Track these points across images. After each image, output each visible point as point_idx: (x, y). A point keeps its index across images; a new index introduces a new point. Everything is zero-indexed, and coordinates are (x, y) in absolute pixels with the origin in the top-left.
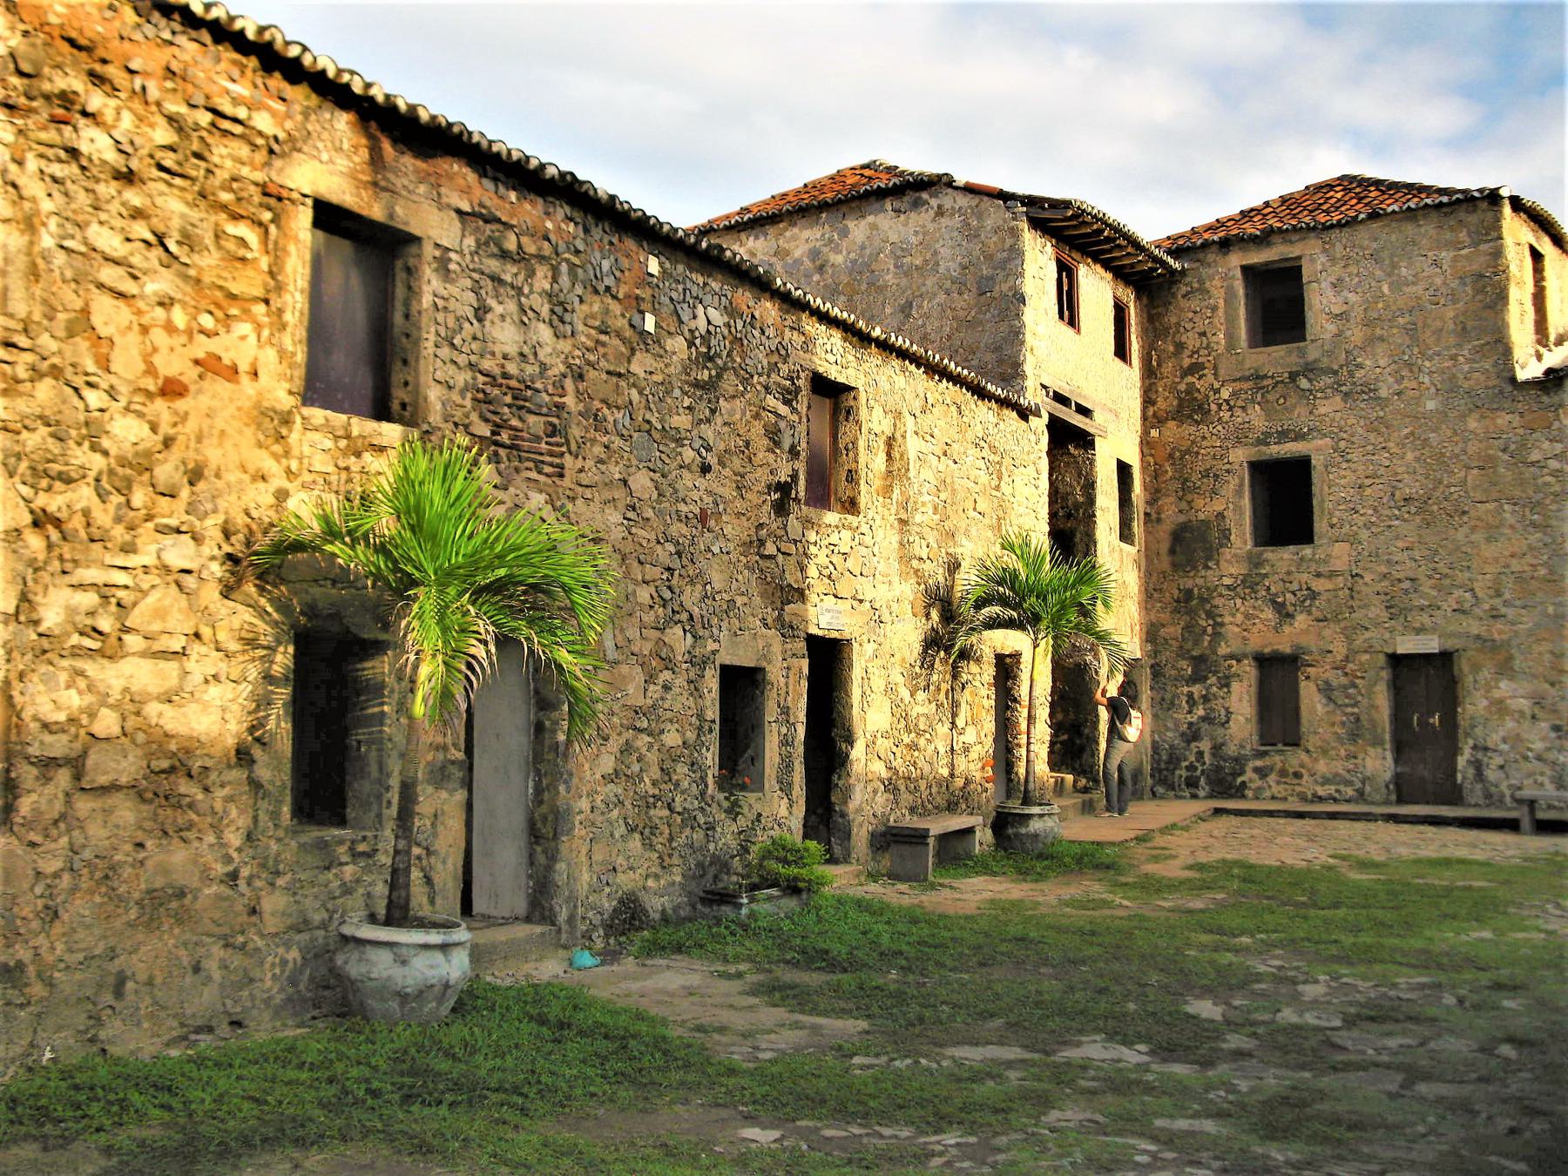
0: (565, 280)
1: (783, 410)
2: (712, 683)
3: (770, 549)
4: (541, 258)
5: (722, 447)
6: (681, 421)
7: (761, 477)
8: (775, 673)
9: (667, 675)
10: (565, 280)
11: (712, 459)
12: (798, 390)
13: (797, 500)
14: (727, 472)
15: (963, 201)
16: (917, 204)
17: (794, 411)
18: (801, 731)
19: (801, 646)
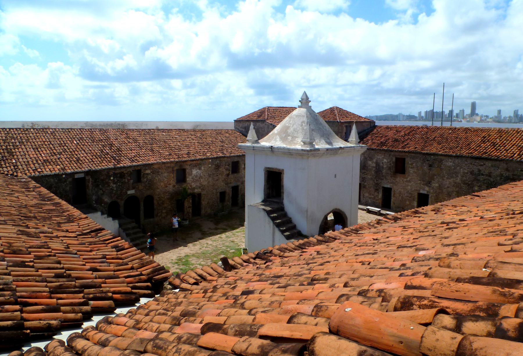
1: (227, 167)
2: (219, 194)
6: (214, 172)
7: (225, 174)
11: (218, 175)
16: (263, 123)
18: (231, 196)
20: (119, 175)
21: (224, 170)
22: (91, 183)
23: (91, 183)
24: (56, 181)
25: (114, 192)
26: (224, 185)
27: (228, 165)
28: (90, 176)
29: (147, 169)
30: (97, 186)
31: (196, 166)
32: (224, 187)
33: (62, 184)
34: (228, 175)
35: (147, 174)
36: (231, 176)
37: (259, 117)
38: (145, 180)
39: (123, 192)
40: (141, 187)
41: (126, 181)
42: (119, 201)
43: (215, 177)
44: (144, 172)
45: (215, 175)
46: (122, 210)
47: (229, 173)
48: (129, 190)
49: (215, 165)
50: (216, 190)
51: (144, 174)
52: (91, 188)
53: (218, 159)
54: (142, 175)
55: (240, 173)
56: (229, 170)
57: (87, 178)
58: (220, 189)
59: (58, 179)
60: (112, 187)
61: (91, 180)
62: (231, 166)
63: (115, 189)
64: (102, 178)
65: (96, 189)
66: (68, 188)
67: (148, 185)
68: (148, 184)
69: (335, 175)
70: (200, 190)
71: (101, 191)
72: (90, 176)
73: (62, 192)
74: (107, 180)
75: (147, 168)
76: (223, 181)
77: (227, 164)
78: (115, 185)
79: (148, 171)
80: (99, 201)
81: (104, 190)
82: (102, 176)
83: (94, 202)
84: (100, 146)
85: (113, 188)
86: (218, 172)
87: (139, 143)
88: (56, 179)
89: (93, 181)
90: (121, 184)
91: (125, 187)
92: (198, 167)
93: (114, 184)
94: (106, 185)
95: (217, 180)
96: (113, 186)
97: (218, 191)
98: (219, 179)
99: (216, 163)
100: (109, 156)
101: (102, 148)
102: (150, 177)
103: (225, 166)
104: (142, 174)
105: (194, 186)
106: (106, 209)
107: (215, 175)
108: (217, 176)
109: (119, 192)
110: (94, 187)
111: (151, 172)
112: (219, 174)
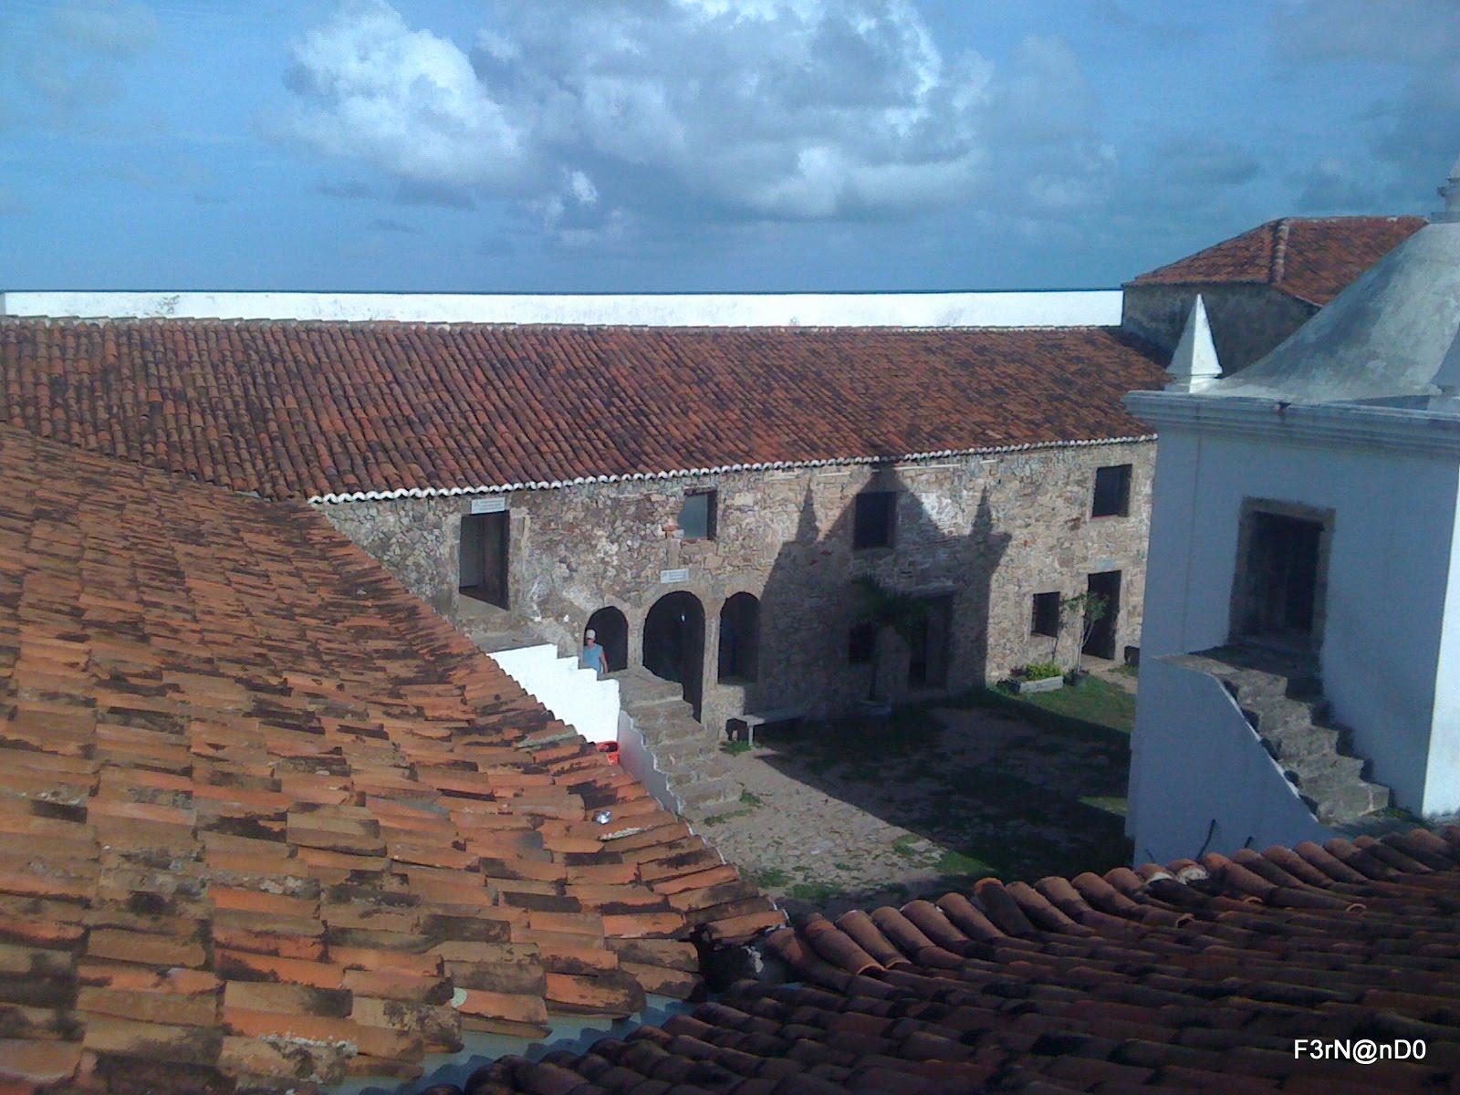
0: (956, 483)
1: (1076, 489)
2: (1028, 603)
3: (1067, 545)
4: (946, 478)
5: (1038, 514)
6: (1017, 511)
7: (1061, 520)
10: (956, 483)
11: (1032, 521)
12: (1086, 479)
13: (1085, 522)
14: (1041, 523)
15: (1279, 297)
17: (1083, 487)
19: (1086, 577)
20: (633, 509)
21: (1060, 503)
22: (527, 533)
23: (527, 533)
24: (405, 521)
25: (611, 572)
26: (1056, 565)
27: (1079, 483)
28: (524, 509)
29: (740, 491)
30: (550, 547)
32: (1055, 576)
33: (425, 533)
34: (1075, 524)
35: (739, 509)
37: (1241, 266)
38: (732, 531)
39: (643, 574)
40: (710, 554)
41: (660, 533)
42: (624, 607)
44: (728, 502)
45: (1019, 522)
46: (635, 643)
47: (1083, 514)
48: (666, 565)
49: (1021, 481)
50: (1020, 587)
51: (728, 507)
52: (525, 552)
53: (1035, 455)
54: (719, 513)
55: (1132, 519)
56: (1083, 505)
57: (516, 515)
58: (1034, 584)
59: (411, 514)
60: (606, 553)
61: (528, 522)
62: (1091, 484)
63: (615, 563)
64: (569, 517)
65: (545, 560)
66: (444, 551)
67: (742, 552)
68: (743, 546)
70: (950, 583)
71: (564, 566)
72: (524, 509)
73: (423, 562)
74: (589, 527)
75: (740, 485)
76: (1051, 549)
77: (1076, 476)
78: (615, 548)
79: (740, 500)
80: (550, 604)
81: (574, 565)
82: (569, 509)
83: (535, 607)
84: (572, 395)
85: (607, 559)
86: (1031, 511)
87: (717, 385)
88: (407, 515)
89: (537, 527)
90: (636, 545)
91: (652, 558)
92: (947, 485)
93: (612, 542)
94: (582, 546)
95: (1026, 543)
96: (608, 548)
97: (1026, 589)
98: (1034, 541)
99: (1028, 473)
100: (603, 435)
101: (577, 402)
102: (753, 519)
103: (1067, 484)
104: (721, 506)
105: (927, 566)
106: (577, 635)
107: (1019, 522)
108: (1028, 525)
109: (629, 573)
110: (538, 552)
111: (756, 503)
112: (1037, 520)
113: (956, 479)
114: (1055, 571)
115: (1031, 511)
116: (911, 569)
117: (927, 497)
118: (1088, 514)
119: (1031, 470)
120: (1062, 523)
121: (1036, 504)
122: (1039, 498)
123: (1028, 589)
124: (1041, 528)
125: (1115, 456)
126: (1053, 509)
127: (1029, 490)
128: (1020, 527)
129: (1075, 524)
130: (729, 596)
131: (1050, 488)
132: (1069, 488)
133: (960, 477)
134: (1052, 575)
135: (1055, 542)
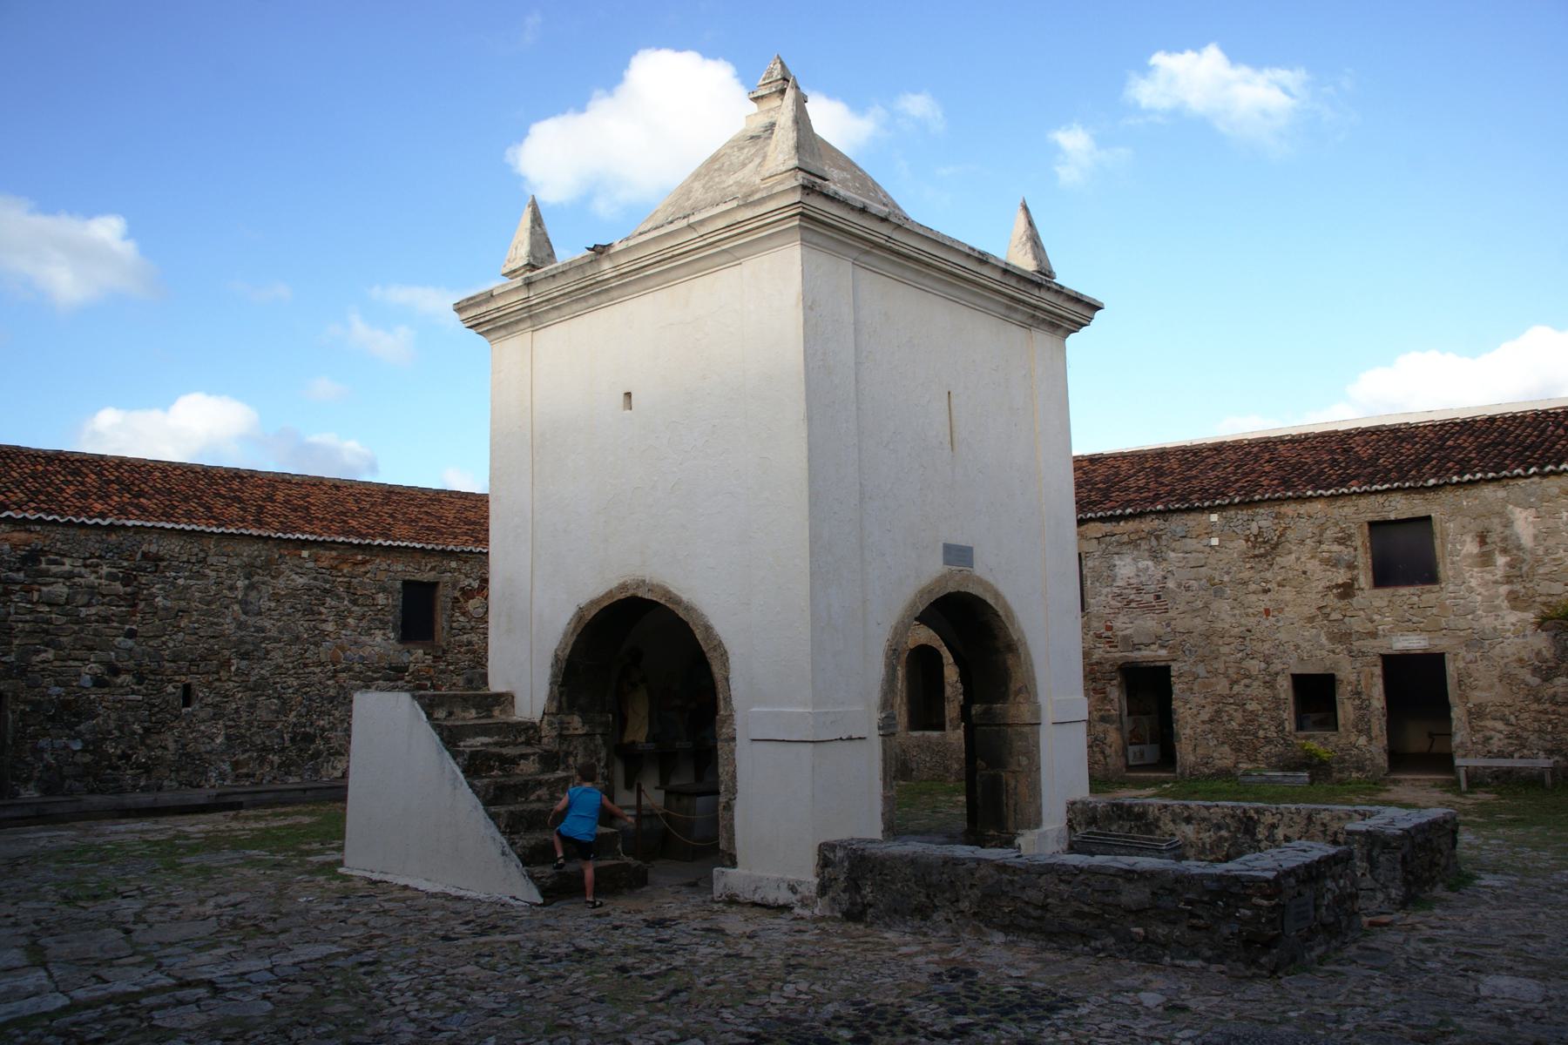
1: (1336, 548)
6: (1246, 575)
8: (1346, 672)
9: (1247, 681)
17: (1347, 546)
21: (1313, 566)
26: (1324, 640)
27: (1343, 540)
31: (1134, 543)
34: (1347, 590)
36: (1371, 598)
43: (1253, 598)
45: (1253, 587)
47: (1354, 579)
56: (1351, 566)
69: (628, 395)
76: (1311, 619)
86: (1269, 575)
95: (1267, 612)
97: (1277, 666)
98: (1281, 610)
99: (1255, 530)
108: (1266, 591)
113: (1153, 538)
114: (1322, 647)
115: (1269, 575)
116: (1109, 633)
117: (1120, 559)
118: (1364, 579)
119: (1260, 528)
120: (1320, 588)
121: (1276, 567)
122: (1278, 559)
123: (1280, 667)
124: (1288, 594)
125: (1400, 507)
126: (1305, 573)
127: (1262, 550)
128: (1254, 593)
129: (1347, 590)
130: (912, 647)
131: (1295, 548)
132: (1325, 547)
133: (1158, 538)
134: (1318, 652)
135: (1314, 611)
